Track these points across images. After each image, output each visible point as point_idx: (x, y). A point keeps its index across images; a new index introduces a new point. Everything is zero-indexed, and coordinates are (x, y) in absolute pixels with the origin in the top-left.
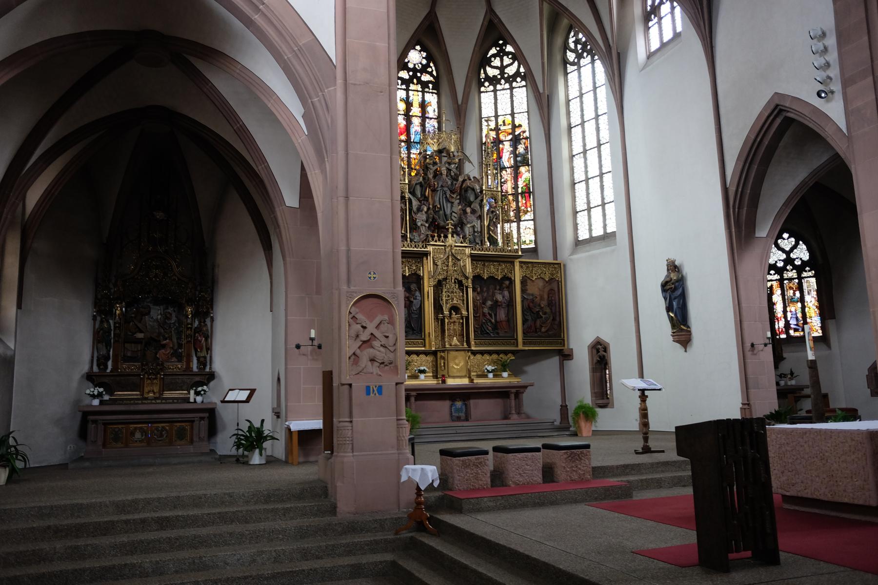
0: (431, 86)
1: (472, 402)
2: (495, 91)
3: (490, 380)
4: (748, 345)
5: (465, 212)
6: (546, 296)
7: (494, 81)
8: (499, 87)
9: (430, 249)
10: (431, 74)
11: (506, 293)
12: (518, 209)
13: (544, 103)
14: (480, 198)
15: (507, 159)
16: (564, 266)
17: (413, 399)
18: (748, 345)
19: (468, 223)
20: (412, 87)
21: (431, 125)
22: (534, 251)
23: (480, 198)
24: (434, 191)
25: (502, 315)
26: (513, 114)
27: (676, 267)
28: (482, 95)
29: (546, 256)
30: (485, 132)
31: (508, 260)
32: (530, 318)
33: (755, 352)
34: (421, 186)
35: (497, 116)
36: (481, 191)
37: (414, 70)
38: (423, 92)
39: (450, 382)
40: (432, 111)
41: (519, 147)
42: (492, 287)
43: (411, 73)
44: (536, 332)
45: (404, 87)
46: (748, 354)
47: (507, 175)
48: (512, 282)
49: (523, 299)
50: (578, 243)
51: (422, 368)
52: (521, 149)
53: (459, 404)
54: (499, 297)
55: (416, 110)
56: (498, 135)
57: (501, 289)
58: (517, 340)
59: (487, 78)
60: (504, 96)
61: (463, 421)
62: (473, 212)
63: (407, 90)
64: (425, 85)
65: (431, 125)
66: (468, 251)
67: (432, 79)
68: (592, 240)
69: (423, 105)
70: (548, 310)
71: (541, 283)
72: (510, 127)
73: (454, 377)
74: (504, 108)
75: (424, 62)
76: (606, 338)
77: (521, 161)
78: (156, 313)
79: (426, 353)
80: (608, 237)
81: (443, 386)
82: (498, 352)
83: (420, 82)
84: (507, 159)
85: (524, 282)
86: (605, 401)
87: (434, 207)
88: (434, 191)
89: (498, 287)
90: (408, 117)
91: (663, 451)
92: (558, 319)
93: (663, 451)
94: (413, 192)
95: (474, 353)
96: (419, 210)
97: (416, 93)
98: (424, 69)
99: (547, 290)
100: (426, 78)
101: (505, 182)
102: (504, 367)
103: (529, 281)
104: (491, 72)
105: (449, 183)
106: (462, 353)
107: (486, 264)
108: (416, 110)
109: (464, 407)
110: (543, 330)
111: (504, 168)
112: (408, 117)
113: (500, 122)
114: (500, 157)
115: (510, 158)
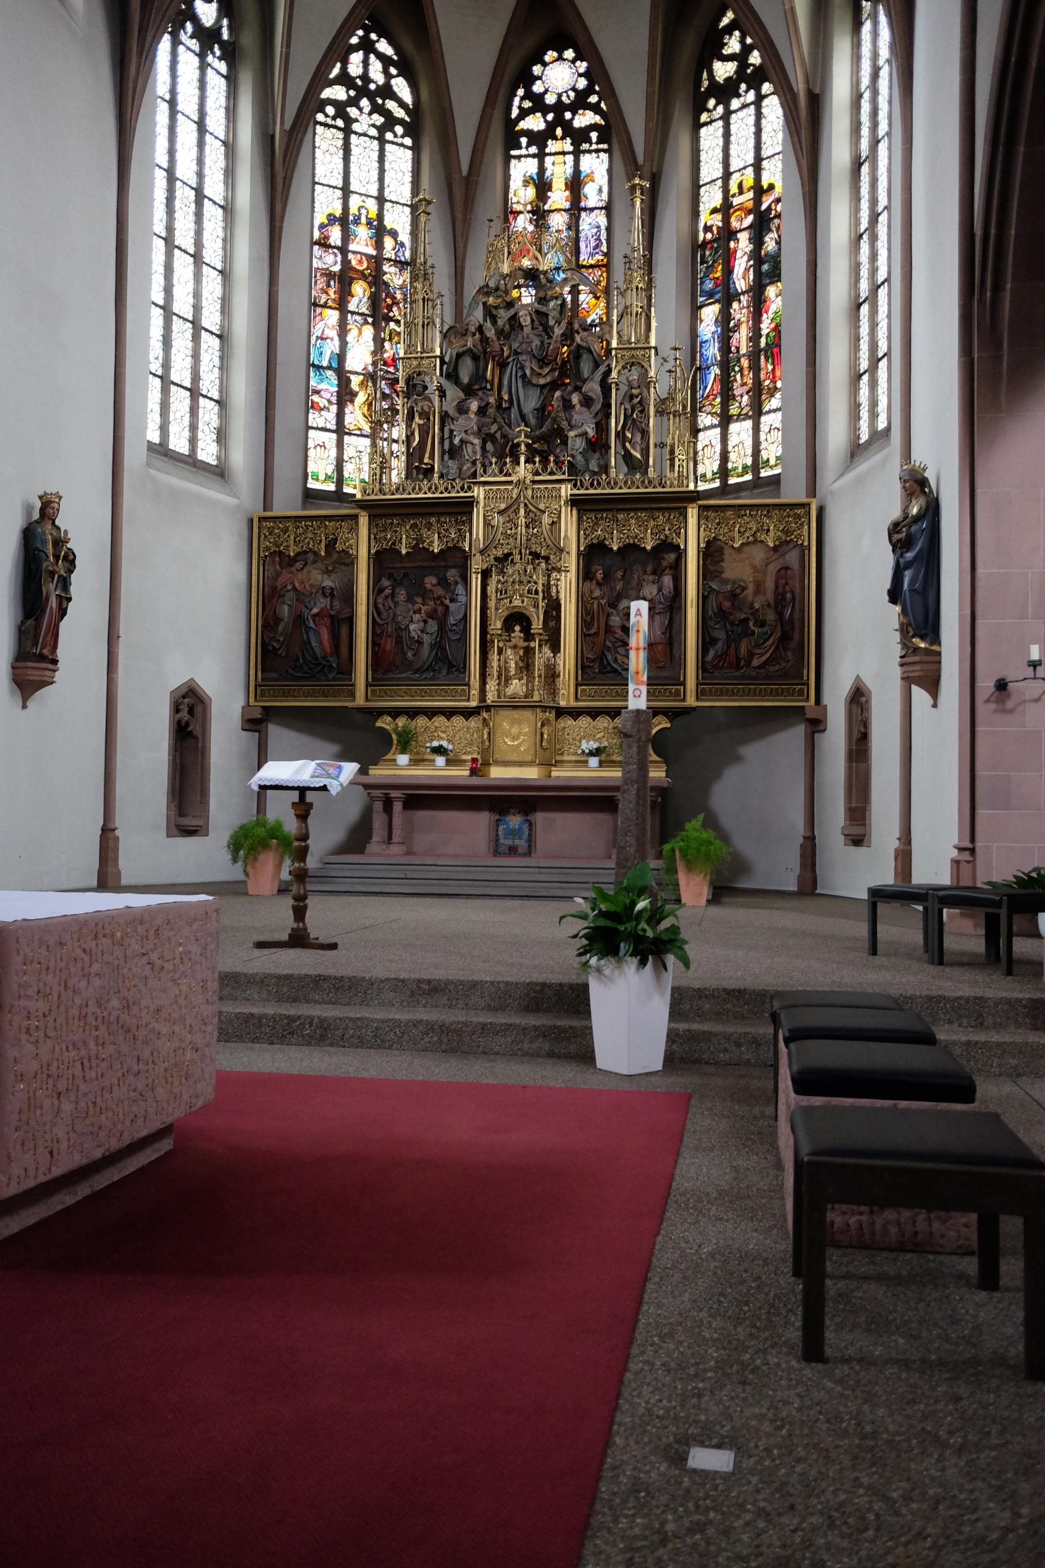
0: (594, 135)
1: (540, 818)
2: (726, 117)
4: (986, 685)
5: (567, 405)
6: (770, 584)
8: (735, 104)
9: (479, 492)
10: (595, 109)
11: (667, 580)
12: (758, 383)
14: (602, 369)
15: (742, 276)
16: (821, 511)
17: (398, 807)
18: (986, 685)
19: (572, 427)
20: (552, 146)
21: (592, 223)
22: (775, 480)
23: (602, 369)
24: (502, 365)
26: (757, 166)
27: (923, 483)
28: (703, 131)
29: (794, 492)
30: (705, 218)
31: (677, 502)
32: (721, 635)
33: (1010, 704)
34: (475, 358)
35: (727, 176)
36: (608, 351)
37: (559, 107)
38: (577, 153)
39: (497, 773)
41: (767, 239)
42: (637, 567)
43: (550, 117)
44: (738, 667)
45: (533, 150)
46: (983, 710)
47: (740, 311)
48: (680, 554)
51: (435, 744)
52: (770, 244)
53: (515, 821)
55: (559, 197)
56: (726, 220)
57: (658, 572)
58: (684, 684)
61: (524, 855)
62: (587, 401)
63: (541, 156)
64: (579, 137)
65: (592, 223)
66: (566, 490)
67: (598, 119)
69: (575, 184)
70: (771, 616)
71: (758, 555)
72: (751, 195)
73: (506, 764)
74: (742, 154)
75: (582, 83)
76: (869, 682)
77: (767, 270)
79: (468, 713)
80: (888, 429)
81: (476, 781)
83: (570, 131)
84: (742, 276)
85: (711, 553)
86: (857, 830)
87: (500, 398)
88: (502, 365)
89: (649, 568)
90: (540, 215)
91: (333, 946)
92: (796, 637)
93: (333, 946)
95: (575, 713)
97: (560, 158)
98: (580, 102)
99: (773, 568)
100: (584, 119)
101: (738, 325)
103: (727, 551)
105: (536, 342)
106: (528, 714)
107: (621, 516)
108: (559, 197)
109: (526, 828)
110: (756, 662)
111: (736, 296)
113: (734, 189)
114: (729, 271)
115: (747, 270)
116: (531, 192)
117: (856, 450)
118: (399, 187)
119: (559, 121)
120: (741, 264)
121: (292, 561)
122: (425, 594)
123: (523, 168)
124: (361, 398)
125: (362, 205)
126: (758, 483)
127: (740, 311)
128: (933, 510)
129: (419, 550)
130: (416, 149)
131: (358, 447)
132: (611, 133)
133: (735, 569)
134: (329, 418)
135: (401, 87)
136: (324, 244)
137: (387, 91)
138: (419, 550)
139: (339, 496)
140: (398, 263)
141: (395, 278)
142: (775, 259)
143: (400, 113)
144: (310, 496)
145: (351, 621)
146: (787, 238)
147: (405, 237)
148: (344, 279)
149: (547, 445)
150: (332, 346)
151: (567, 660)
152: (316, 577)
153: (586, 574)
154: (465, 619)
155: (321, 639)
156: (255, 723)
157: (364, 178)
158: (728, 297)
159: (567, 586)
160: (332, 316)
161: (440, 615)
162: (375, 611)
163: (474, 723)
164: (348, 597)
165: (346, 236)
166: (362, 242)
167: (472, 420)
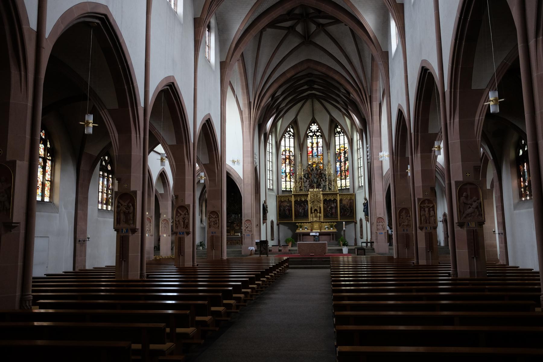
3: (327, 230)
5: (321, 181)
7: (339, 133)
13: (351, 142)
15: (343, 159)
20: (314, 138)
22: (349, 189)
25: (334, 211)
26: (344, 144)
29: (351, 192)
30: (337, 150)
31: (336, 194)
37: (314, 132)
40: (320, 144)
47: (343, 164)
48: (337, 201)
49: (340, 207)
50: (359, 187)
54: (333, 205)
55: (315, 145)
59: (337, 132)
60: (342, 138)
62: (323, 180)
64: (318, 136)
65: (320, 149)
66: (321, 192)
68: (362, 186)
69: (317, 143)
71: (347, 200)
74: (342, 142)
77: (346, 159)
78: (233, 216)
79: (309, 223)
82: (331, 222)
84: (343, 159)
85: (341, 200)
90: (312, 148)
94: (304, 176)
95: (323, 222)
96: (306, 181)
98: (317, 131)
100: (318, 134)
102: (332, 226)
104: (339, 130)
108: (315, 145)
112: (312, 148)
116: (311, 144)
117: (359, 187)
118: (292, 145)
119: (314, 134)
120: (342, 158)
121: (282, 202)
122: (302, 206)
123: (309, 141)
124: (288, 176)
125: (287, 148)
126: (346, 189)
127: (343, 164)
128: (367, 202)
129: (301, 200)
130: (294, 139)
131: (288, 183)
132: (322, 136)
133: (344, 202)
134: (284, 180)
135: (292, 130)
136: (283, 155)
137: (290, 131)
138: (301, 200)
139: (286, 191)
140: (293, 156)
141: (292, 158)
142: (347, 158)
143: (292, 134)
144: (283, 191)
145: (292, 210)
146: (348, 155)
147: (293, 152)
148: (285, 159)
149: (318, 186)
150: (284, 169)
151: (322, 215)
152: (286, 204)
153: (324, 203)
154: (308, 210)
155: (287, 212)
156: (278, 225)
157: (287, 145)
158: (341, 162)
159: (322, 205)
160: (284, 165)
161: (304, 209)
162: (295, 208)
163: (310, 224)
164: (291, 206)
165: (286, 153)
166: (287, 154)
167: (308, 183)
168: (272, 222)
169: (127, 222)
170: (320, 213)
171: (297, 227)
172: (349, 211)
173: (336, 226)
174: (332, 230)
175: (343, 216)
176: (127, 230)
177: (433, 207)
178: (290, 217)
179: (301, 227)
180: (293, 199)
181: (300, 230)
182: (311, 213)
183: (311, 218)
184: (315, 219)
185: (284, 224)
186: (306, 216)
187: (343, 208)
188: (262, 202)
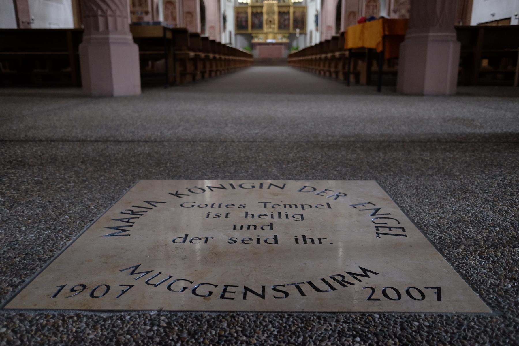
3: (280, 41)
25: (287, 22)
29: (303, 5)
31: (289, 6)
66: (277, 5)
85: (294, 13)
102: (284, 37)
144: (240, 3)
151: (276, 26)
155: (244, 24)
156: (236, 34)
159: (276, 17)
164: (247, 18)
168: (230, 33)
169: (140, 5)
170: (274, 24)
171: (252, 38)
172: (300, 23)
173: (289, 38)
174: (285, 40)
175: (295, 27)
176: (142, 13)
177: (376, 6)
178: (245, 27)
179: (257, 37)
180: (249, 11)
181: (256, 40)
182: (267, 24)
183: (265, 28)
184: (270, 30)
185: (242, 34)
186: (261, 26)
187: (296, 21)
188: (222, 11)
